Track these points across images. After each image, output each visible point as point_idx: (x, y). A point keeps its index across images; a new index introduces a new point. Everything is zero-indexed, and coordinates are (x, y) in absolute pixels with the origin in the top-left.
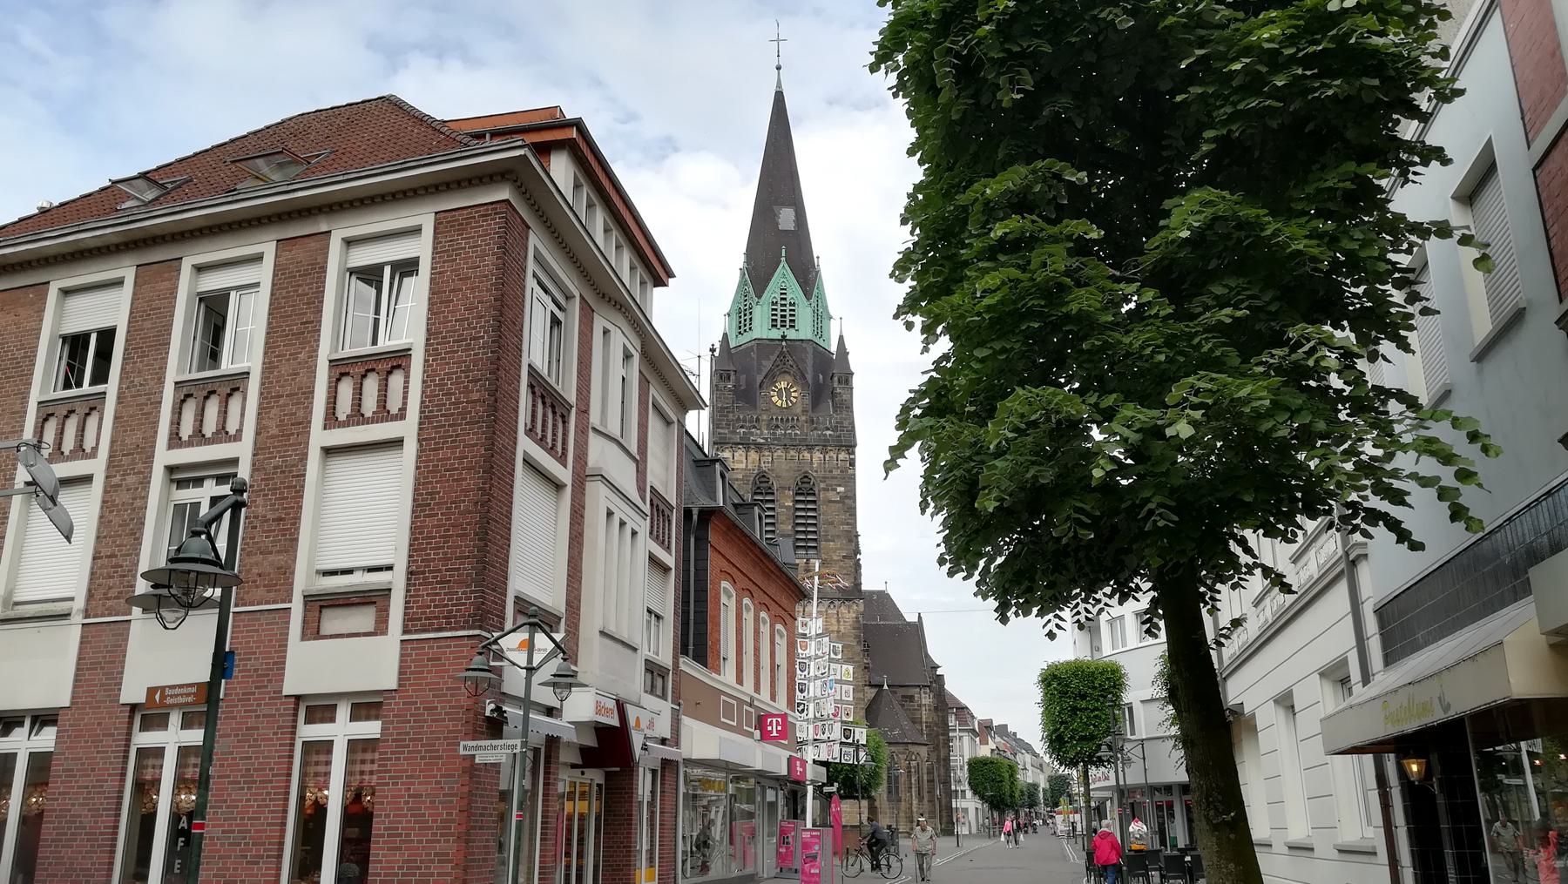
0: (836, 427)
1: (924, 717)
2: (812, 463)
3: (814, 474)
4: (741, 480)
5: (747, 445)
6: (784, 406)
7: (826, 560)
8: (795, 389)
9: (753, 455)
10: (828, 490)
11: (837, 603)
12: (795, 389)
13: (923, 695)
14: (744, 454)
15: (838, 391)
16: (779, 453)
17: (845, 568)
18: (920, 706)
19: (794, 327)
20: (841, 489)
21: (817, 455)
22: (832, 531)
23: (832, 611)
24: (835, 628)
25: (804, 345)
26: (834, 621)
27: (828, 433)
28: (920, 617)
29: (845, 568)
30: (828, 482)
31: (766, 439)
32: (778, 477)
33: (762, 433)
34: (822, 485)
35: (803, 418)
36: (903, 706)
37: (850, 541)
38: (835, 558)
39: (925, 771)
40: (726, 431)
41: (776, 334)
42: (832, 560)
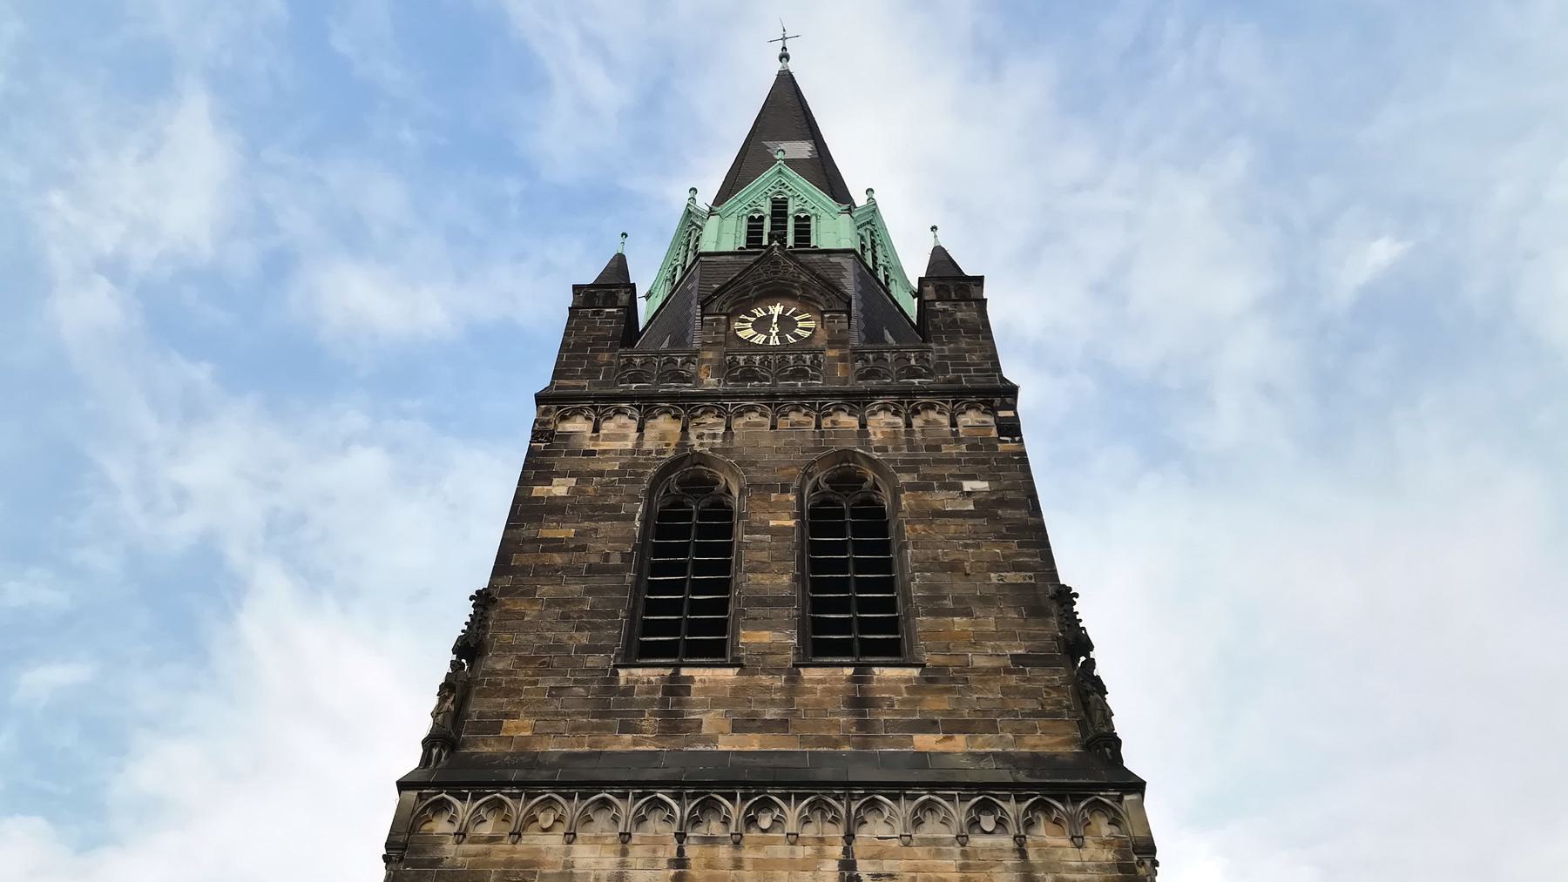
4: (612, 473)
7: (940, 669)
10: (928, 488)
14: (634, 425)
22: (954, 586)
23: (992, 842)
29: (1028, 694)
30: (923, 469)
37: (1036, 612)
38: (980, 662)
42: (966, 667)
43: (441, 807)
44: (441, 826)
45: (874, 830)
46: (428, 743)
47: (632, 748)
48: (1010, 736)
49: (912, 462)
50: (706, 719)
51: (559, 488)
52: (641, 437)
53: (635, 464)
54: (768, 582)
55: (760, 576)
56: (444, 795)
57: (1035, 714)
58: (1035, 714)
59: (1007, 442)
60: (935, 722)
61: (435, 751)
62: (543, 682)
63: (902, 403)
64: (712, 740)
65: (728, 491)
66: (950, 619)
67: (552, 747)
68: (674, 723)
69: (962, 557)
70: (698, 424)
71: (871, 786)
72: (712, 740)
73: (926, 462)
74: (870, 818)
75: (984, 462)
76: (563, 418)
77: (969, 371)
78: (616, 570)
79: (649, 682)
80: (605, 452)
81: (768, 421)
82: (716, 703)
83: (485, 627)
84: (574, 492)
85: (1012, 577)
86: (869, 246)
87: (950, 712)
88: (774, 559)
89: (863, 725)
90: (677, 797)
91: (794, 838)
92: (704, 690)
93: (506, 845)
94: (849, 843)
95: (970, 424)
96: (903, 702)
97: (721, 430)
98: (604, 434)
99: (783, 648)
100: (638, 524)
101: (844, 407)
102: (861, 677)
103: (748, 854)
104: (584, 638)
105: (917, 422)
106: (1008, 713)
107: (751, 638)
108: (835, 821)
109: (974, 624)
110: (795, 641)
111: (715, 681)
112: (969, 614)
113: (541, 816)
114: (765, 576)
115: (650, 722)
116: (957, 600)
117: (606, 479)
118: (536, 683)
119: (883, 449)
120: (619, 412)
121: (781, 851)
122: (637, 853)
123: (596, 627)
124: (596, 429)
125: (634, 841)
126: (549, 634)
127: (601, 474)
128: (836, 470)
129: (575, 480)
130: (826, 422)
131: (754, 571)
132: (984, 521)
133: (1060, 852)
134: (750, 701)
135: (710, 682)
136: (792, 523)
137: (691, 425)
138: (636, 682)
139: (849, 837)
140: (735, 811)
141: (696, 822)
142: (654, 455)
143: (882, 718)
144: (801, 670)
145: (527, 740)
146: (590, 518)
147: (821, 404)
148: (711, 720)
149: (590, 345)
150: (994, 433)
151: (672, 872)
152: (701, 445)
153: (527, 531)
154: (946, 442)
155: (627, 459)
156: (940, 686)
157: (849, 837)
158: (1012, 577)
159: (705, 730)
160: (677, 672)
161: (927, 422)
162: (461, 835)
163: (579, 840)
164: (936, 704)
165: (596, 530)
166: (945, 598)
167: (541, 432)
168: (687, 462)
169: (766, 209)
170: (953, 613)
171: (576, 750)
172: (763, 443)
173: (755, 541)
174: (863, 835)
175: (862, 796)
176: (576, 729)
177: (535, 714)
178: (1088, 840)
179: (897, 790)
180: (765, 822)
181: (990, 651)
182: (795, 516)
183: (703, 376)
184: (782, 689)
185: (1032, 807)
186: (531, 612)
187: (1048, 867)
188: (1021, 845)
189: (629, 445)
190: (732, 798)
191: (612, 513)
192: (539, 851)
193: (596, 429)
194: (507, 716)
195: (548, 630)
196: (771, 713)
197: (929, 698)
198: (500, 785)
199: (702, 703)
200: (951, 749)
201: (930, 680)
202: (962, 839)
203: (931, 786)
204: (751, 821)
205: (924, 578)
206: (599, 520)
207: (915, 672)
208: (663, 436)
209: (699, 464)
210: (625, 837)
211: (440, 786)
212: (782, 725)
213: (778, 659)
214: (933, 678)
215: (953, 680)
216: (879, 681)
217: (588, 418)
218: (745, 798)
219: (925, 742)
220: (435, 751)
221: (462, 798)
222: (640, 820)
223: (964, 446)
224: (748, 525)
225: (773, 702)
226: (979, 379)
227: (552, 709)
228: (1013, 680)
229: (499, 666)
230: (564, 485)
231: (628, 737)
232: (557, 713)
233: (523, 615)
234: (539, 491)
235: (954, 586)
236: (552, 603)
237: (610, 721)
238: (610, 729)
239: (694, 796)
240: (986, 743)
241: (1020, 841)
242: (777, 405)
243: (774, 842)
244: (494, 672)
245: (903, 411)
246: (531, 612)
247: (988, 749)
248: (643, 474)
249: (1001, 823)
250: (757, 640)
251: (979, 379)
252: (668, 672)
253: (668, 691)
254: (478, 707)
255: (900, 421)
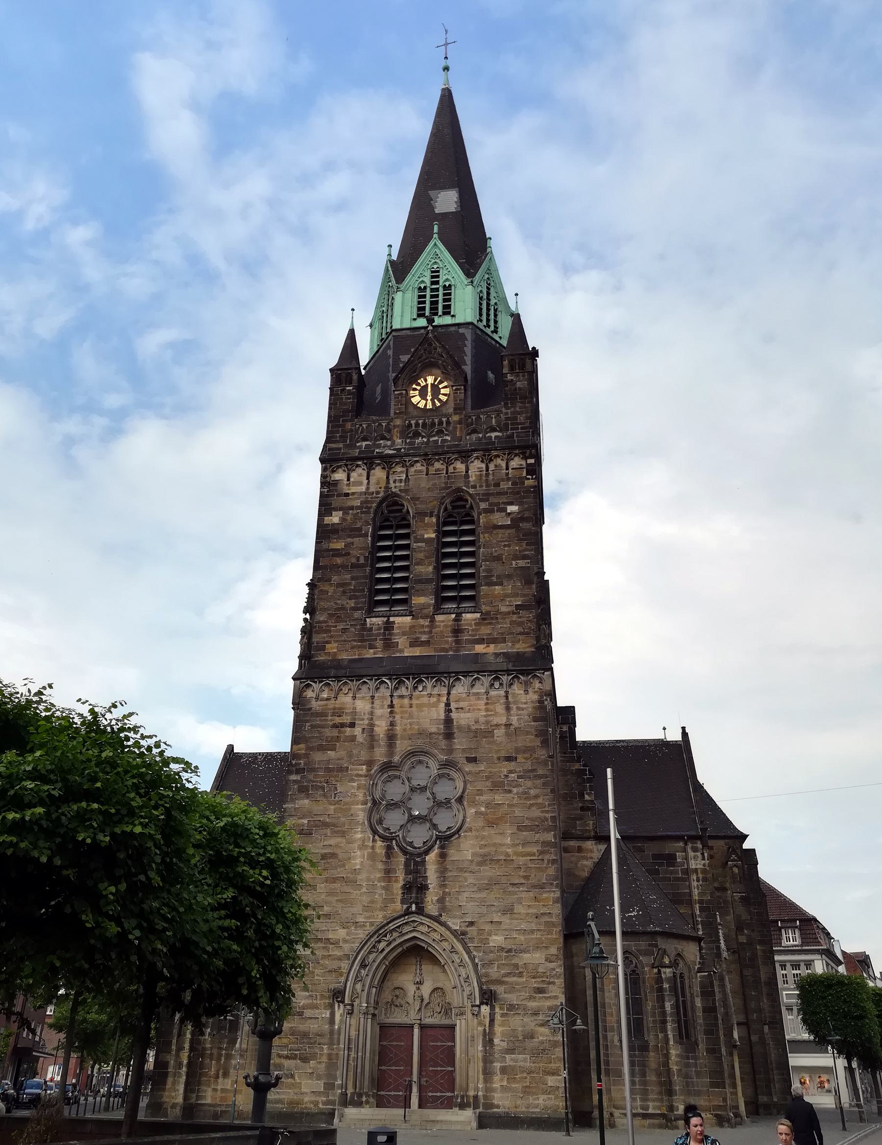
0: (506, 425)
1: (696, 892)
2: (467, 476)
3: (471, 491)
4: (357, 508)
5: (370, 461)
6: (429, 406)
7: (488, 613)
8: (445, 384)
9: (379, 473)
11: (505, 679)
12: (445, 384)
13: (691, 854)
14: (365, 473)
15: (509, 377)
16: (418, 467)
17: (520, 624)
18: (687, 872)
19: (449, 313)
20: (512, 509)
21: (476, 466)
22: (498, 569)
23: (498, 693)
24: (503, 720)
25: (461, 331)
26: (500, 708)
27: (493, 435)
28: (685, 734)
29: (520, 624)
30: (492, 500)
31: (399, 450)
32: (415, 499)
33: (393, 443)
34: (483, 505)
35: (456, 418)
36: (653, 872)
37: (528, 582)
38: (504, 609)
39: (697, 989)
40: (341, 445)
41: (422, 322)
42: (498, 612)
43: (308, 686)
44: (309, 694)
45: (460, 689)
46: (301, 657)
47: (373, 656)
48: (510, 644)
49: (488, 495)
50: (400, 641)
51: (335, 518)
52: (368, 483)
53: (366, 502)
54: (423, 571)
55: (420, 567)
56: (309, 682)
57: (521, 634)
58: (521, 634)
59: (529, 479)
60: (484, 639)
61: (303, 662)
62: (339, 626)
63: (485, 456)
64: (402, 651)
65: (408, 512)
66: (494, 587)
67: (344, 656)
68: (389, 644)
69: (502, 552)
70: (394, 472)
71: (457, 673)
72: (402, 651)
73: (492, 494)
74: (457, 684)
75: (518, 493)
76: (333, 471)
77: (518, 429)
78: (362, 566)
79: (378, 625)
80: (353, 494)
81: (424, 468)
82: (404, 634)
83: (314, 599)
84: (343, 519)
85: (522, 563)
86: (485, 297)
87: (490, 634)
88: (427, 557)
89: (457, 642)
90: (390, 679)
91: (430, 695)
92: (399, 628)
93: (332, 701)
94: (449, 696)
95: (515, 467)
96: (473, 630)
97: (404, 477)
98: (353, 482)
99: (429, 605)
100: (370, 539)
101: (459, 459)
102: (458, 619)
103: (414, 702)
104: (352, 603)
105: (492, 467)
106: (512, 633)
107: (418, 600)
108: (444, 686)
109: (503, 590)
110: (433, 602)
111: (403, 623)
112: (502, 585)
113: (343, 689)
114: (422, 567)
115: (379, 643)
116: (498, 577)
117: (355, 512)
118: (336, 626)
119: (474, 487)
120: (358, 466)
121: (425, 700)
122: (377, 702)
123: (356, 597)
124: (348, 480)
125: (375, 698)
126: (339, 602)
127: (352, 508)
128: (454, 497)
129: (341, 512)
130: (451, 469)
131: (418, 564)
132: (513, 531)
133: (519, 696)
134: (416, 632)
135: (401, 623)
136: (433, 536)
137: (390, 473)
138: (373, 624)
139: (449, 694)
140: (409, 684)
141: (396, 688)
142: (375, 495)
143: (464, 638)
144: (435, 616)
145: (335, 653)
146: (350, 536)
147: (449, 458)
148: (402, 641)
149: (342, 416)
150: (524, 474)
151: (389, 710)
152: (395, 487)
153: (325, 545)
154: (503, 480)
155: (363, 498)
156: (486, 622)
157: (449, 694)
158: (522, 563)
159: (400, 647)
160: (389, 619)
161: (496, 466)
162: (317, 699)
163: (357, 698)
164: (485, 630)
165: (352, 543)
166: (493, 576)
167: (326, 483)
168: (390, 497)
169: (427, 280)
170: (496, 584)
171: (353, 657)
172: (423, 485)
173: (419, 547)
174: (453, 692)
175: (454, 676)
176: (353, 648)
177: (337, 641)
178: (530, 690)
179: (466, 674)
180: (420, 688)
181: (508, 604)
182: (435, 531)
183: (395, 438)
184: (427, 626)
185: (513, 678)
186: (331, 590)
187: (515, 703)
188: (507, 694)
189: (363, 488)
190: (408, 679)
191: (356, 532)
192: (344, 703)
193: (348, 480)
194: (328, 642)
195: (339, 600)
196: (424, 638)
197: (482, 628)
198: (328, 678)
199: (398, 634)
200: (488, 652)
201: (484, 619)
202: (487, 693)
203: (478, 672)
204: (415, 688)
205: (486, 565)
206: (354, 537)
207: (478, 615)
208: (378, 483)
209: (395, 497)
210: (373, 697)
211: (307, 679)
212: (427, 643)
213: (426, 611)
214: (486, 618)
215: (492, 618)
216: (465, 620)
217: (344, 471)
218: (414, 679)
219: (480, 648)
220: (303, 662)
221: (315, 682)
222: (377, 689)
223: (510, 483)
224: (415, 538)
225: (424, 633)
226: (522, 435)
227: (343, 639)
228: (515, 617)
229: (321, 619)
230: (337, 516)
231: (372, 651)
232: (345, 641)
233: (328, 592)
234: (327, 520)
235: (498, 569)
236: (339, 585)
237: (364, 644)
238: (364, 647)
239: (396, 679)
240: (502, 648)
241: (507, 692)
242: (429, 459)
243: (423, 696)
244: (320, 622)
245: (485, 461)
246: (331, 590)
247: (502, 651)
248: (370, 507)
249: (501, 684)
250: (419, 602)
251: (522, 435)
252: (385, 619)
253: (386, 629)
254: (316, 638)
255: (483, 466)
